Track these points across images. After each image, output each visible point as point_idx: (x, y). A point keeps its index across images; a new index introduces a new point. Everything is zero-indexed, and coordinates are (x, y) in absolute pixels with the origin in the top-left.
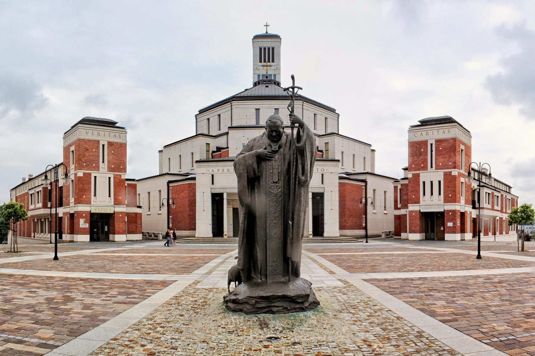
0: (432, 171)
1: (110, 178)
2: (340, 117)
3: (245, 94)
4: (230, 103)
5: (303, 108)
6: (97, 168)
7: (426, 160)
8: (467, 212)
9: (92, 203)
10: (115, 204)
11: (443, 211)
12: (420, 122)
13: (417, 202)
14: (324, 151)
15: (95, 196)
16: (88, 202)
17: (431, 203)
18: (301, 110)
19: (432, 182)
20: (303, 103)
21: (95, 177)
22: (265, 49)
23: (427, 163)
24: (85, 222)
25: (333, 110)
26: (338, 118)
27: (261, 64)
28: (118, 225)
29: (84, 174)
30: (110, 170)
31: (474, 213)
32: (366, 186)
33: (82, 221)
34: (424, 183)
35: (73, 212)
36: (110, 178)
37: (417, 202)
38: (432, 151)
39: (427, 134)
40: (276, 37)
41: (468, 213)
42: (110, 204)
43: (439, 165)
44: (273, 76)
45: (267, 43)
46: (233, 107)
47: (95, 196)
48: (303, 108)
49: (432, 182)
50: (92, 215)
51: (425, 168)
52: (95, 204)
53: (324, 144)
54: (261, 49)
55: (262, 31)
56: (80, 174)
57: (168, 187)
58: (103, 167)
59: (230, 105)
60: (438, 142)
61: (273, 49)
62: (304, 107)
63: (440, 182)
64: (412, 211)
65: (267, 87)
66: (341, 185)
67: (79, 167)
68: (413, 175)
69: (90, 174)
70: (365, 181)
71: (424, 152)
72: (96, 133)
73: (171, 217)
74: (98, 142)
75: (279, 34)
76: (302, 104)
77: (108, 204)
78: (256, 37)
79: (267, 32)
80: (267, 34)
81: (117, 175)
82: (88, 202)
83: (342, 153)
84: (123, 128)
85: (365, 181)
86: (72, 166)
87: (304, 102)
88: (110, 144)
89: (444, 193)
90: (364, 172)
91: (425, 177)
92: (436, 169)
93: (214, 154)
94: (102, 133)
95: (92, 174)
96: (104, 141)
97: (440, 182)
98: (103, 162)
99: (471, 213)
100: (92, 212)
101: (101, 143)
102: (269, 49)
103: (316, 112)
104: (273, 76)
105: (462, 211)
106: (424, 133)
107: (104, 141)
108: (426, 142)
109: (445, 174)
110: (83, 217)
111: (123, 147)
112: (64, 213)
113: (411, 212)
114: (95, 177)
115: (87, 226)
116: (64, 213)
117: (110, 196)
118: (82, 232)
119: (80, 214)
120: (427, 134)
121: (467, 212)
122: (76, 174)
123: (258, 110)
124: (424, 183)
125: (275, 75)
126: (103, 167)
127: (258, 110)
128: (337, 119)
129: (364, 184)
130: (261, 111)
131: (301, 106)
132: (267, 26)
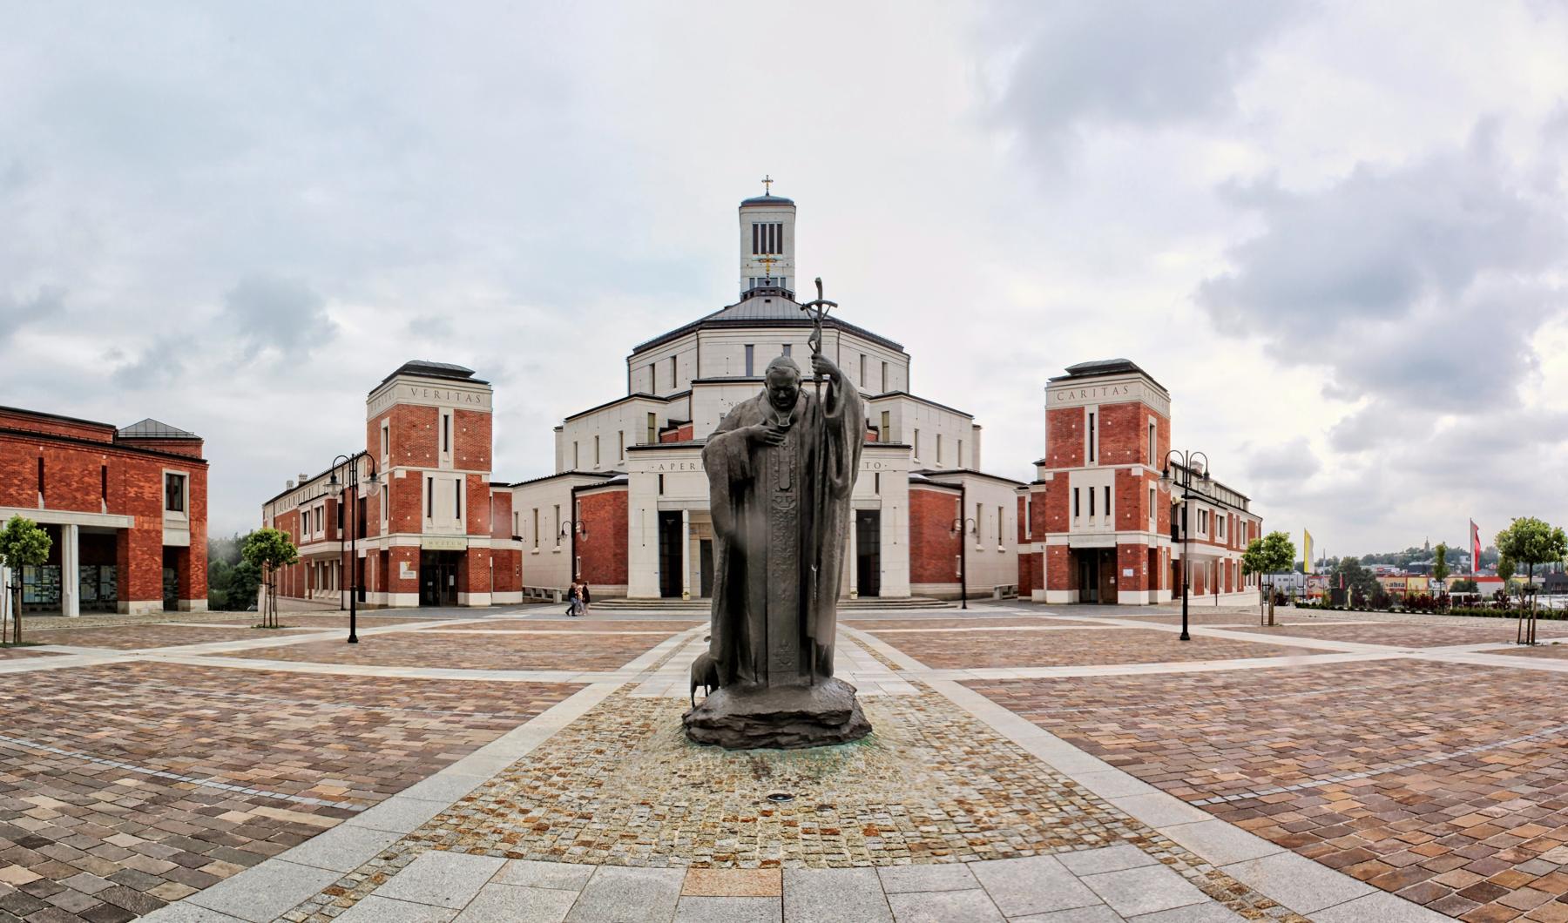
0: (1091, 467)
1: (458, 481)
2: (911, 361)
3: (726, 316)
6: (434, 462)
7: (1080, 446)
8: (1161, 548)
9: (424, 530)
10: (469, 533)
11: (1114, 546)
12: (1068, 370)
13: (1064, 528)
14: (880, 429)
15: (430, 516)
16: (417, 529)
17: (1092, 531)
18: (836, 347)
19: (1092, 489)
21: (430, 480)
22: (764, 226)
23: (1083, 452)
24: (410, 568)
25: (897, 348)
26: (908, 363)
27: (756, 257)
28: (476, 574)
29: (408, 473)
30: (460, 465)
31: (1176, 551)
32: (962, 497)
33: (404, 566)
34: (1077, 490)
35: (387, 549)
36: (458, 481)
37: (1064, 528)
38: (1092, 428)
39: (1083, 395)
40: (786, 203)
41: (1164, 549)
42: (459, 533)
43: (1108, 457)
44: (779, 280)
45: (768, 216)
47: (430, 516)
49: (1092, 489)
50: (424, 553)
51: (1079, 462)
52: (430, 532)
53: (880, 415)
54: (755, 226)
55: (759, 193)
56: (401, 473)
57: (574, 499)
58: (446, 459)
60: (1105, 410)
61: (780, 226)
62: (841, 341)
63: (1108, 489)
64: (1053, 546)
65: (768, 301)
66: (914, 495)
67: (398, 459)
68: (1056, 475)
69: (420, 474)
70: (960, 487)
71: (1076, 430)
72: (431, 392)
73: (578, 557)
74: (436, 410)
75: (791, 198)
76: (836, 335)
77: (454, 531)
78: (747, 204)
79: (767, 194)
80: (767, 198)
81: (472, 475)
82: (417, 529)
83: (916, 431)
84: (485, 383)
85: (960, 487)
86: (385, 459)
88: (459, 414)
89: (1116, 510)
90: (960, 469)
91: (1079, 478)
92: (1100, 464)
93: (663, 434)
94: (442, 393)
95: (424, 474)
96: (447, 409)
97: (1108, 489)
98: (446, 450)
99: (1169, 550)
100: (423, 548)
101: (442, 412)
102: (772, 226)
103: (864, 351)
104: (779, 280)
105: (1151, 546)
106: (1077, 393)
107: (447, 409)
108: (1079, 412)
109: (1119, 474)
110: (405, 559)
111: (484, 419)
112: (368, 551)
113: (1051, 548)
114: (430, 480)
115: (414, 575)
116: (368, 551)
117: (458, 517)
118: (405, 587)
119: (401, 553)
120: (1083, 395)
121: (1161, 548)
122: (392, 474)
123: (750, 347)
124: (1077, 490)
125: (783, 279)
126: (446, 459)
127: (750, 347)
128: (905, 364)
129: (958, 493)
130: (757, 350)
131: (835, 339)
132: (767, 181)
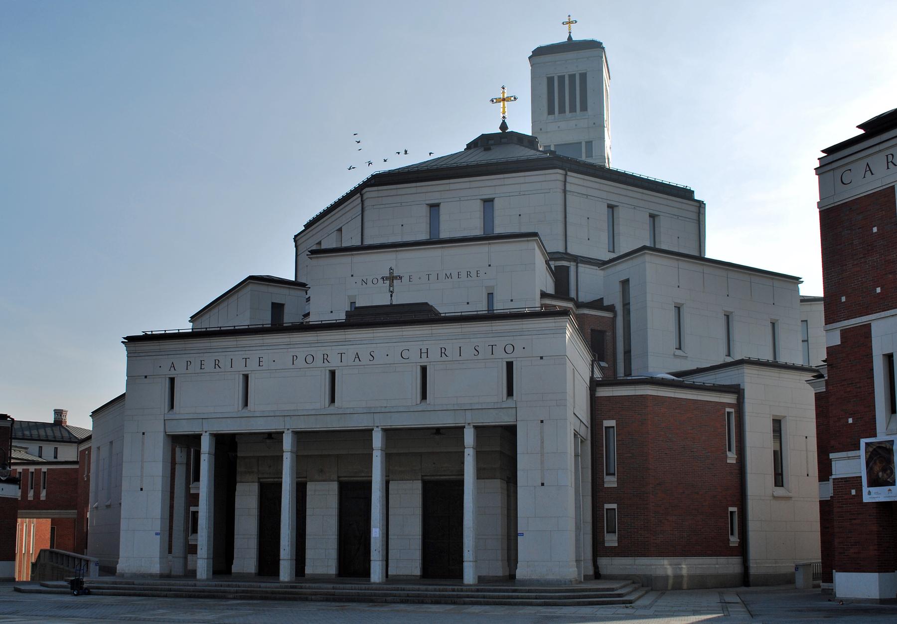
4: (359, 195)
5: (565, 191)
20: (566, 175)
40: (595, 46)
44: (583, 145)
45: (568, 65)
46: (366, 203)
48: (565, 191)
54: (550, 80)
59: (360, 199)
61: (583, 76)
62: (568, 187)
75: (598, 39)
76: (561, 178)
78: (539, 52)
87: (569, 173)
90: (729, 360)
103: (614, 199)
104: (583, 145)
125: (589, 144)
129: (730, 399)
130: (443, 209)
131: (560, 185)
